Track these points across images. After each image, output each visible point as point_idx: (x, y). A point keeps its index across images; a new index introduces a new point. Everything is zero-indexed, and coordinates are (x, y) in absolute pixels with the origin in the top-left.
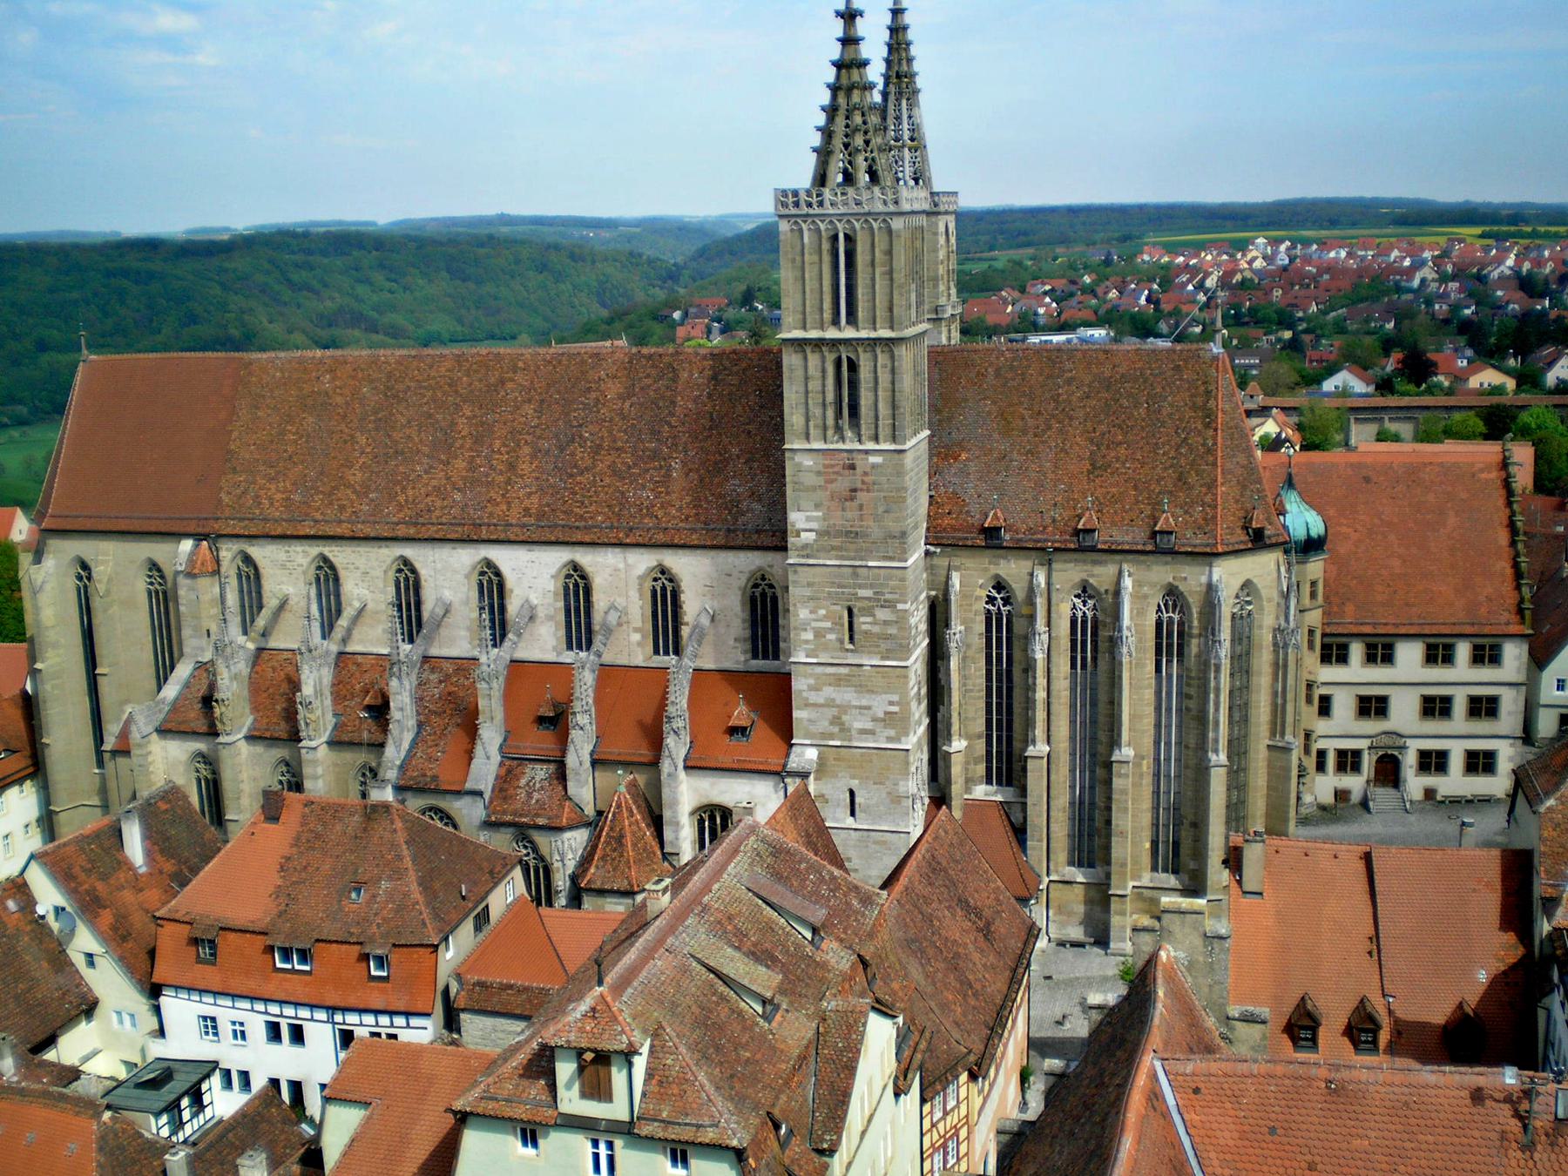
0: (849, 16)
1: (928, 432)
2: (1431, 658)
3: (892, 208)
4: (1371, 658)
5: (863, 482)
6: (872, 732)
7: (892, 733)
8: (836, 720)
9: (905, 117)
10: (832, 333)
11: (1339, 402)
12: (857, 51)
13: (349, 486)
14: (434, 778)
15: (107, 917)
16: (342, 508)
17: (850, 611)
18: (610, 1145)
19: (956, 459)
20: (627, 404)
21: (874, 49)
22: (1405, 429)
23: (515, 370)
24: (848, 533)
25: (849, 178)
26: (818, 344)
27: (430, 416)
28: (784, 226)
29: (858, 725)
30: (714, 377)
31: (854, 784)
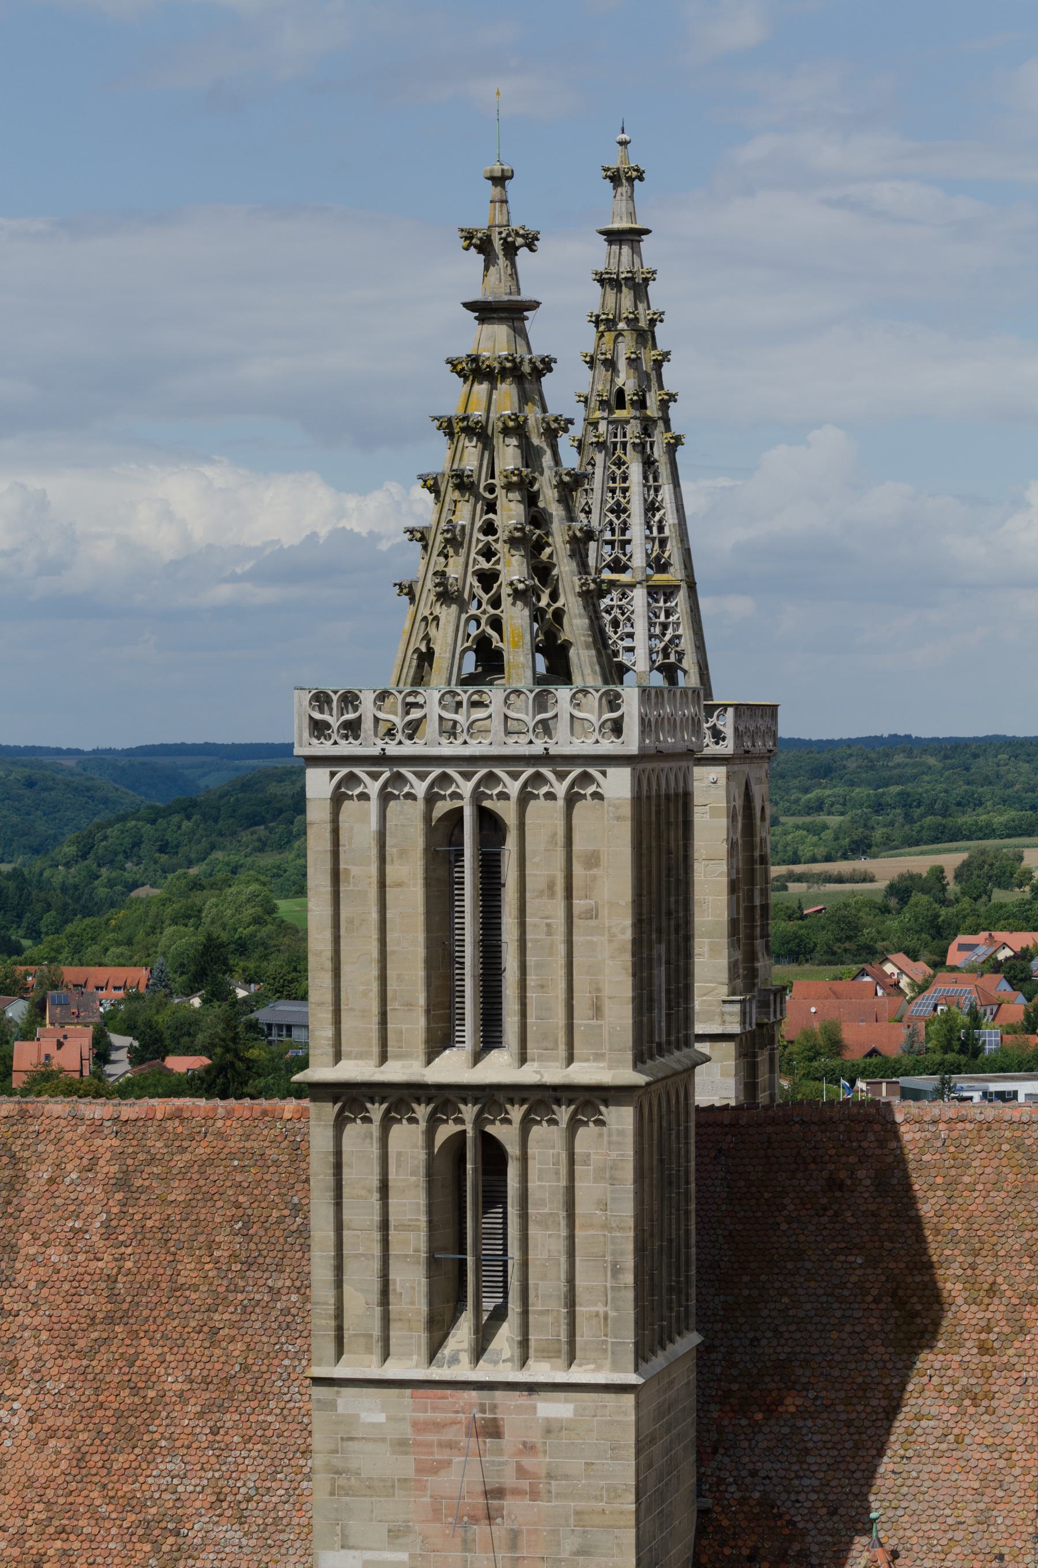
1: (692, 1339)
3: (608, 746)
5: (521, 1472)
9: (636, 508)
12: (520, 333)
25: (490, 662)
26: (400, 1098)
28: (319, 784)
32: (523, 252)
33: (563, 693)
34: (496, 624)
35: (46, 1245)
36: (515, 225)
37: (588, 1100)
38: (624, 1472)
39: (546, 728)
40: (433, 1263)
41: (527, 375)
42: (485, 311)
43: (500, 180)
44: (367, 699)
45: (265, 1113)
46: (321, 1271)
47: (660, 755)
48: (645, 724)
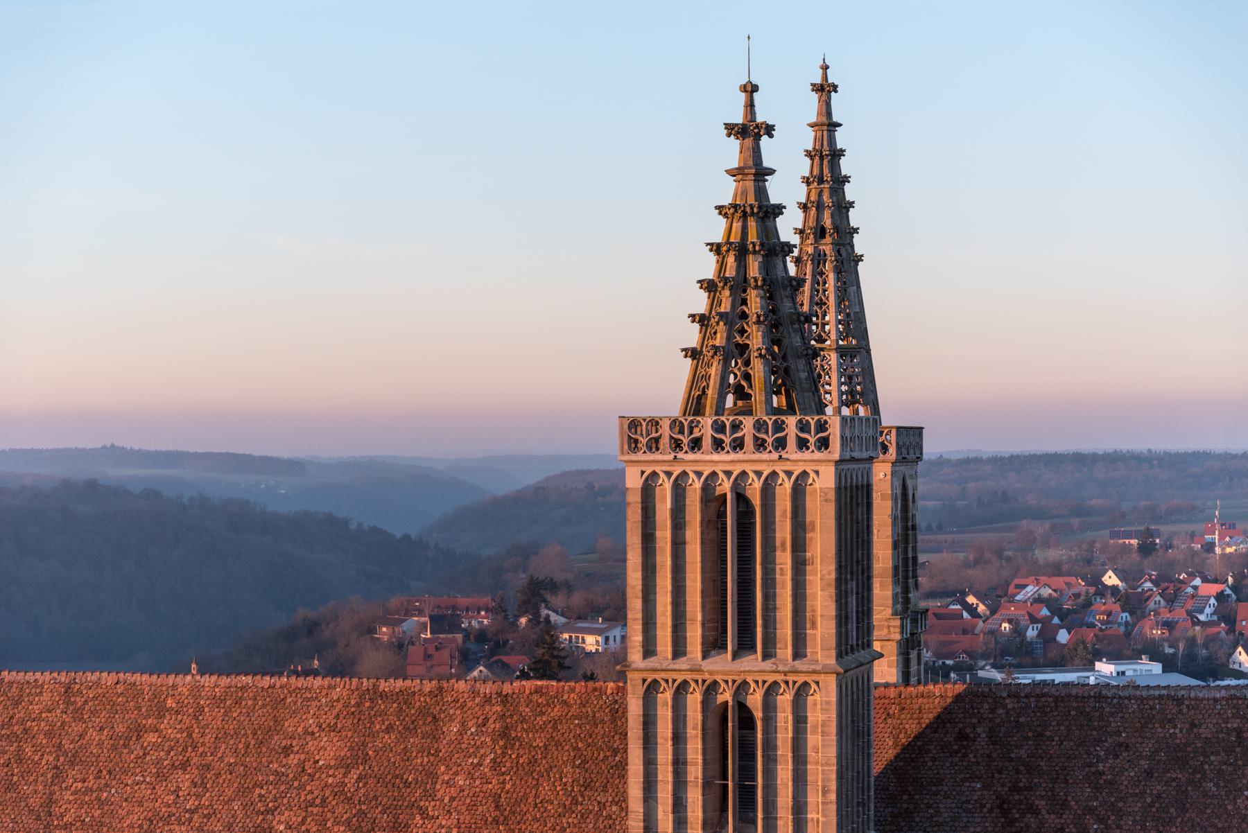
0: (750, 132)
20: (354, 775)
21: (788, 188)
23: (161, 711)
30: (504, 733)
32: (765, 138)
34: (747, 377)
35: (456, 773)
36: (759, 119)
40: (706, 785)
43: (750, 89)
44: (665, 425)
45: (595, 689)
47: (853, 460)
48: (843, 438)
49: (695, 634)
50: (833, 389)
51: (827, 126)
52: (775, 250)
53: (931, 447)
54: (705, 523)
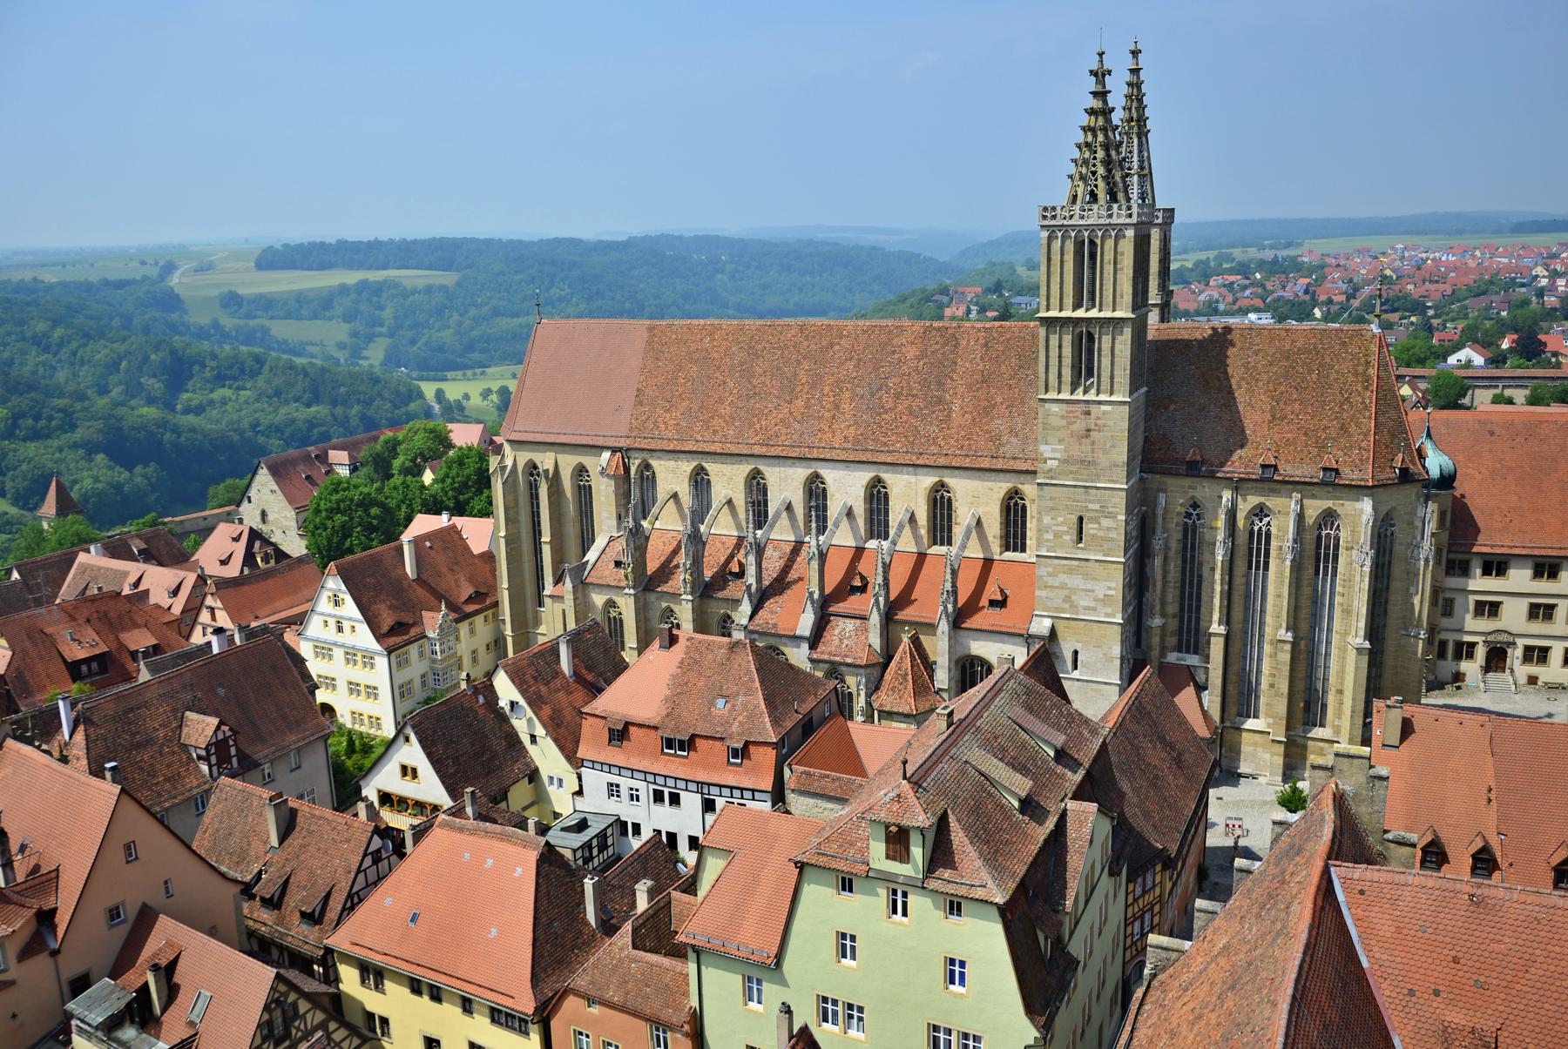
0: (1100, 75)
2: (1538, 574)
3: (1128, 221)
4: (1487, 572)
6: (1094, 609)
7: (1109, 610)
8: (1067, 599)
10: (1080, 313)
11: (1463, 373)
12: (1105, 102)
13: (721, 417)
14: (775, 625)
15: (547, 711)
16: (715, 432)
17: (1081, 519)
18: (905, 895)
19: (1166, 408)
21: (1117, 100)
22: (1520, 395)
24: (1082, 462)
25: (1094, 197)
27: (779, 369)
29: (1083, 603)
30: (986, 345)
31: (1078, 647)
33: (1115, 206)
37: (1117, 323)
38: (1125, 425)
39: (1110, 216)
41: (1106, 112)
42: (1095, 94)
43: (1101, 55)
46: (1042, 369)
47: (1143, 223)
49: (1069, 301)
50: (1135, 193)
51: (1135, 71)
52: (1108, 127)
53: (1177, 218)
54: (1075, 252)
